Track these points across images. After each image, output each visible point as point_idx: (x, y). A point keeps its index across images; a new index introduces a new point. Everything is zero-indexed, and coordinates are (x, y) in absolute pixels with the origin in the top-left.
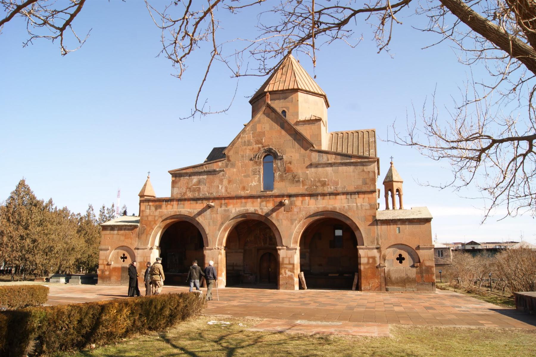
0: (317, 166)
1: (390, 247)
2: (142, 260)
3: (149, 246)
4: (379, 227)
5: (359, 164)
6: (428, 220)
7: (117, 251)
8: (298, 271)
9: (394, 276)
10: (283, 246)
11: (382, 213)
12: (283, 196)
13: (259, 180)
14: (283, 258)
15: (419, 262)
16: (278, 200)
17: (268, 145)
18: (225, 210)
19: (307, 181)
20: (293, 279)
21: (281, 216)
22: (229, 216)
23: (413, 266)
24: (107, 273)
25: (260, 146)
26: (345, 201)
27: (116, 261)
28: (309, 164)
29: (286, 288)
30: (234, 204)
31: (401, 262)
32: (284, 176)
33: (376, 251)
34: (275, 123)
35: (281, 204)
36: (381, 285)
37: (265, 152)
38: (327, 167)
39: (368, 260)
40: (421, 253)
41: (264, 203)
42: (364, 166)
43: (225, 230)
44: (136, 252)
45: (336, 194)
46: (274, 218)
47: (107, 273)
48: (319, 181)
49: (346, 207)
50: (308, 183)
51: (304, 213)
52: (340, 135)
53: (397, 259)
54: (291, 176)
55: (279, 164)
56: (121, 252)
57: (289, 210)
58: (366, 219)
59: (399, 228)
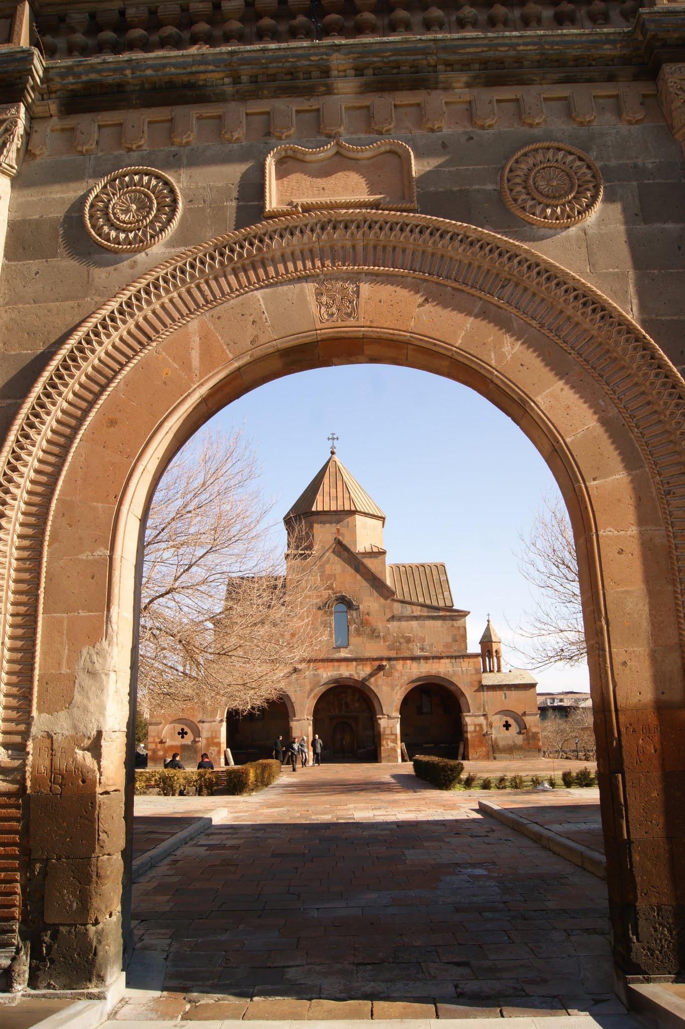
0: (400, 619)
1: (496, 714)
2: (209, 735)
3: (218, 718)
4: (485, 693)
5: (448, 618)
6: (533, 686)
7: (173, 725)
8: (399, 742)
9: (501, 743)
10: (383, 714)
11: (489, 679)
12: (382, 659)
13: (331, 635)
14: (384, 728)
15: (526, 728)
16: (377, 663)
17: (340, 592)
18: (314, 675)
19: (388, 636)
20: (396, 751)
21: (380, 682)
22: (319, 681)
23: (520, 733)
24: (161, 753)
25: (330, 592)
26: (449, 665)
27: (173, 739)
28: (390, 615)
29: (389, 761)
30: (324, 668)
31: (507, 729)
32: (361, 629)
33: (482, 718)
34: (348, 564)
35: (381, 668)
36: (488, 754)
37: (337, 600)
38: (412, 620)
39: (475, 728)
40: (527, 719)
41: (360, 667)
42: (453, 620)
43: (314, 697)
44: (200, 725)
45: (440, 658)
46: (372, 683)
47: (161, 753)
48: (403, 637)
49: (451, 672)
50: (390, 638)
51: (405, 678)
52: (402, 569)
53: (504, 726)
54: (369, 629)
55: (355, 615)
56: (178, 727)
57: (389, 675)
58: (472, 685)
59: (505, 694)
